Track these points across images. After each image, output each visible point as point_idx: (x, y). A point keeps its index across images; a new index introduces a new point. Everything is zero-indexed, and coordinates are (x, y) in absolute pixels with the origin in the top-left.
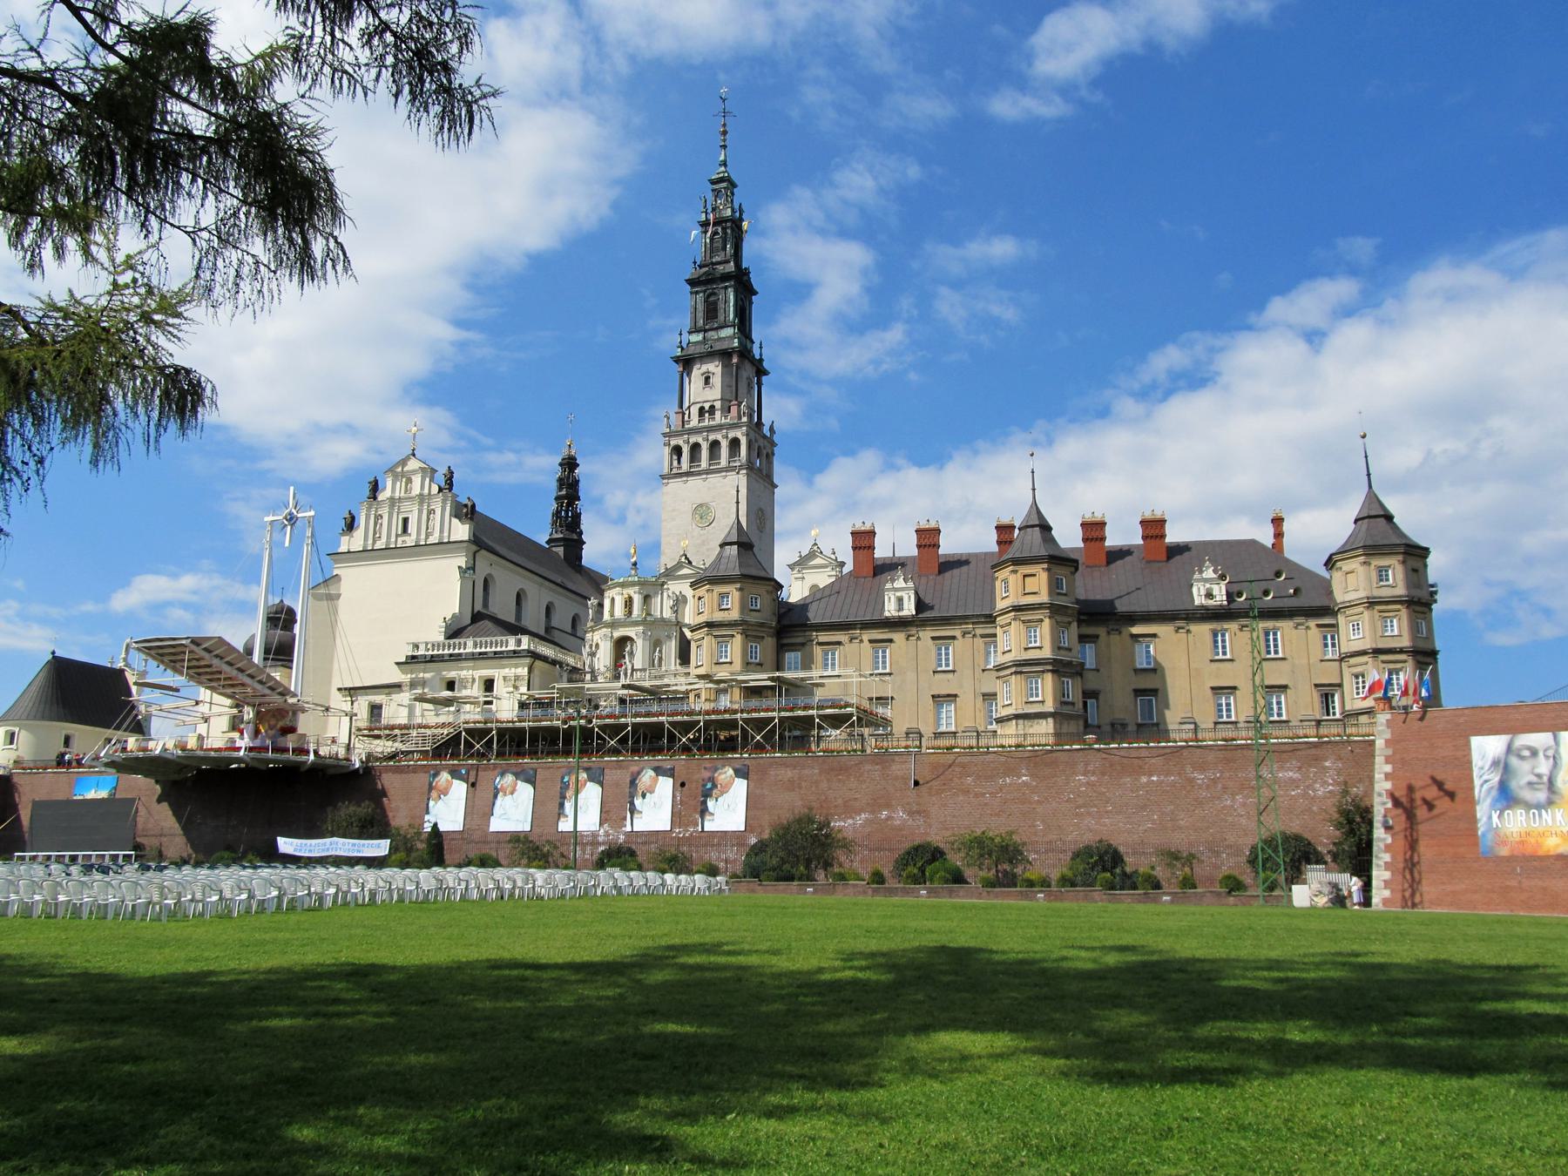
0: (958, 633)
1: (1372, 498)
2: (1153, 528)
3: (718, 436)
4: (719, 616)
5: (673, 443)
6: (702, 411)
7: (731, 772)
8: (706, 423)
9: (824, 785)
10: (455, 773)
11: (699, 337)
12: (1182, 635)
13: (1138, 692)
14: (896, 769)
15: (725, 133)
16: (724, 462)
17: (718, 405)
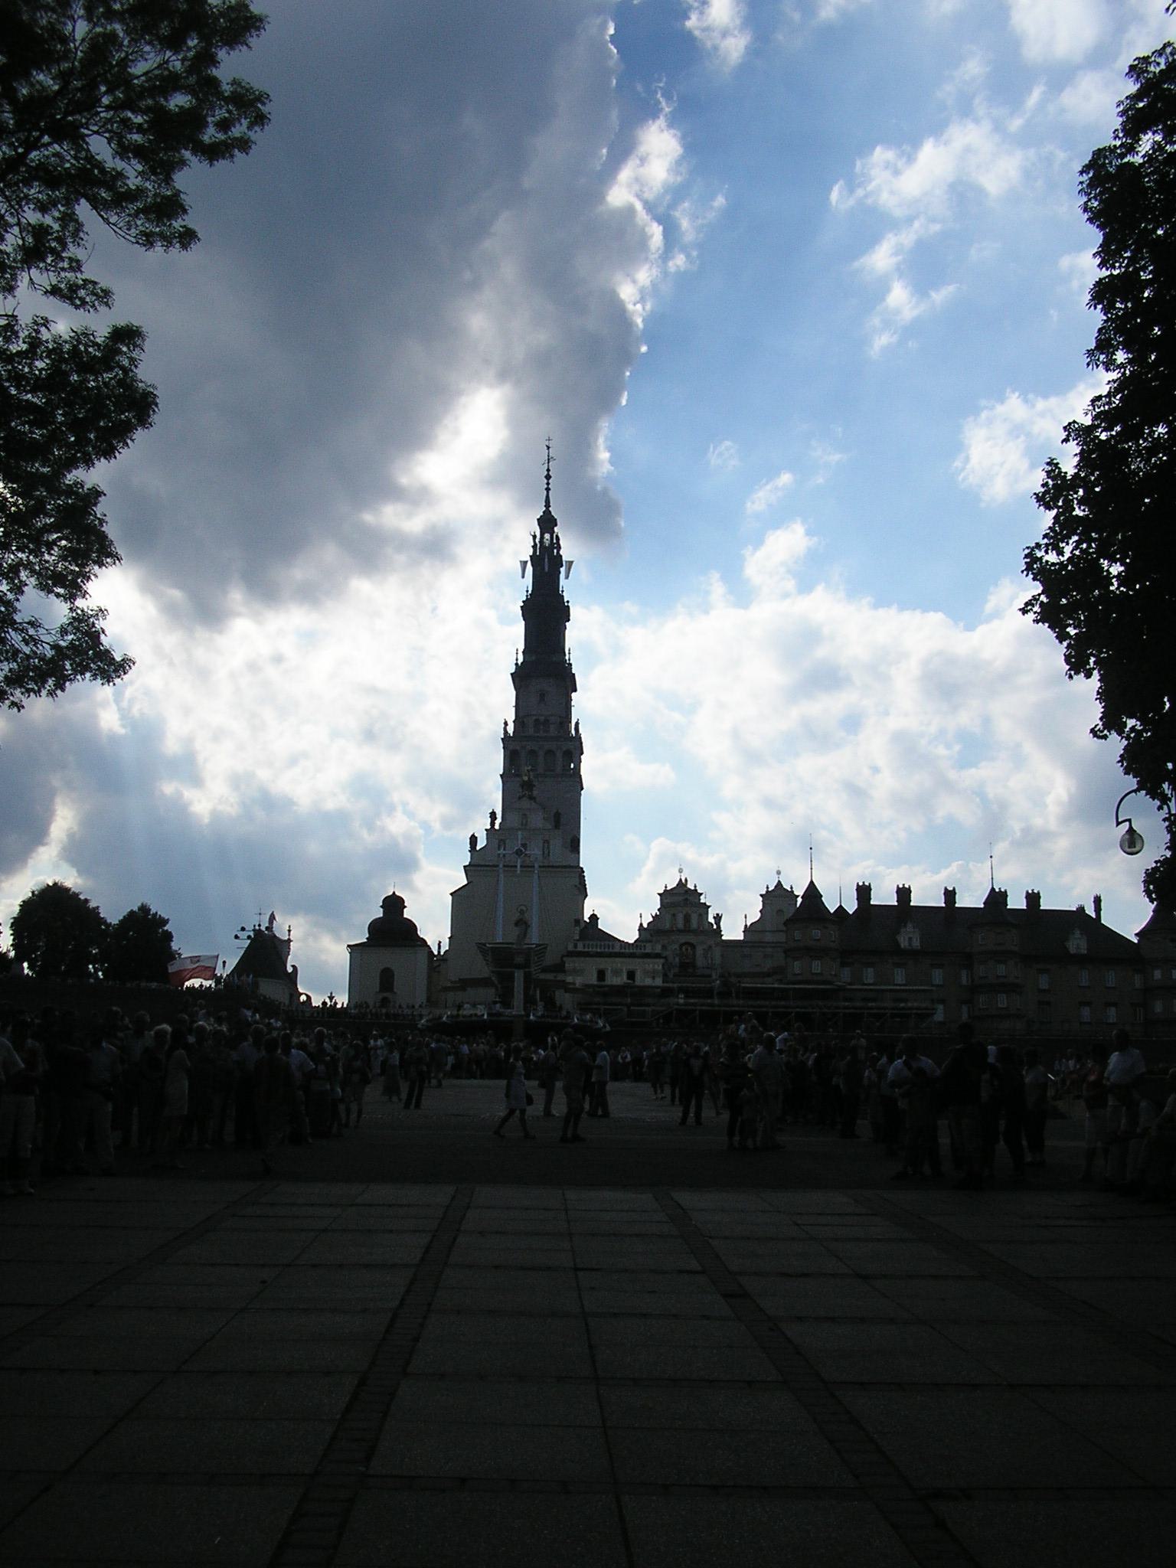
2: (1033, 898)
8: (542, 734)
15: (548, 477)
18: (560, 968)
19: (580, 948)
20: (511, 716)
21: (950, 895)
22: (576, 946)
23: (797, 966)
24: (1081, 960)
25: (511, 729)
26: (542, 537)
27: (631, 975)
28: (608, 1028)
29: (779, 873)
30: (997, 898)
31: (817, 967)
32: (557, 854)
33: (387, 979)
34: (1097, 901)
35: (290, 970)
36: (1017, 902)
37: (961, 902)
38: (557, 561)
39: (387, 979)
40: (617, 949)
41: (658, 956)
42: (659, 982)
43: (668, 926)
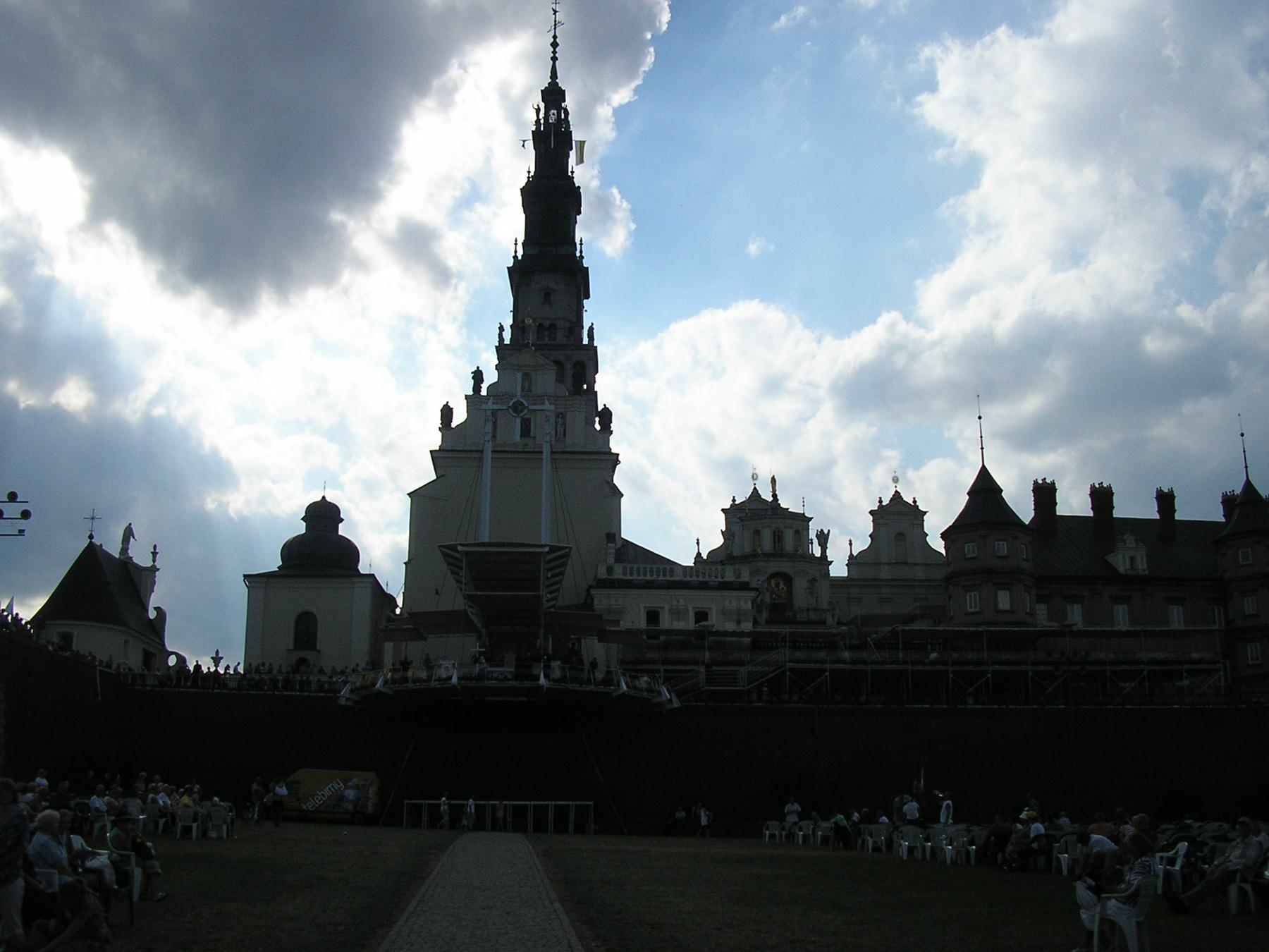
15: (555, 45)
19: (618, 573)
20: (508, 321)
21: (1166, 500)
22: (610, 570)
23: (972, 601)
27: (701, 616)
28: (676, 704)
29: (896, 480)
31: (1004, 600)
33: (306, 629)
35: (152, 614)
37: (1182, 513)
39: (306, 629)
40: (678, 577)
41: (744, 586)
42: (747, 626)
43: (748, 550)
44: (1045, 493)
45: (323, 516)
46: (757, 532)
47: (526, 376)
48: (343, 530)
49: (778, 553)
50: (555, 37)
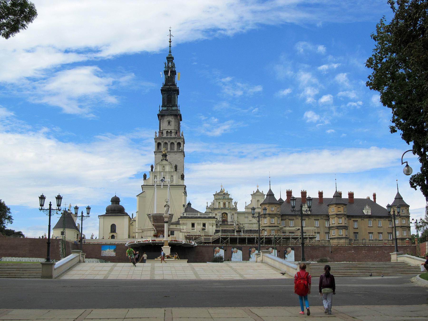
0: (320, 218)
1: (398, 194)
2: (351, 195)
3: (173, 141)
4: (271, 212)
5: (158, 141)
6: (167, 132)
7: (290, 249)
8: (169, 136)
9: (311, 252)
10: (220, 248)
11: (165, 108)
12: (363, 221)
13: (354, 233)
14: (327, 249)
15: (170, 42)
16: (176, 150)
17: (173, 131)
18: (177, 223)
19: (185, 215)
21: (321, 194)
22: (183, 215)
24: (369, 217)
25: (158, 135)
26: (168, 64)
30: (338, 195)
32: (176, 180)
33: (113, 228)
34: (374, 196)
35: (77, 225)
36: (345, 196)
37: (324, 196)
38: (174, 73)
39: (113, 228)
40: (199, 215)
41: (214, 218)
43: (217, 207)
44: (289, 193)
45: (116, 200)
46: (219, 203)
47: (164, 167)
48: (121, 204)
49: (224, 208)
50: (170, 39)
